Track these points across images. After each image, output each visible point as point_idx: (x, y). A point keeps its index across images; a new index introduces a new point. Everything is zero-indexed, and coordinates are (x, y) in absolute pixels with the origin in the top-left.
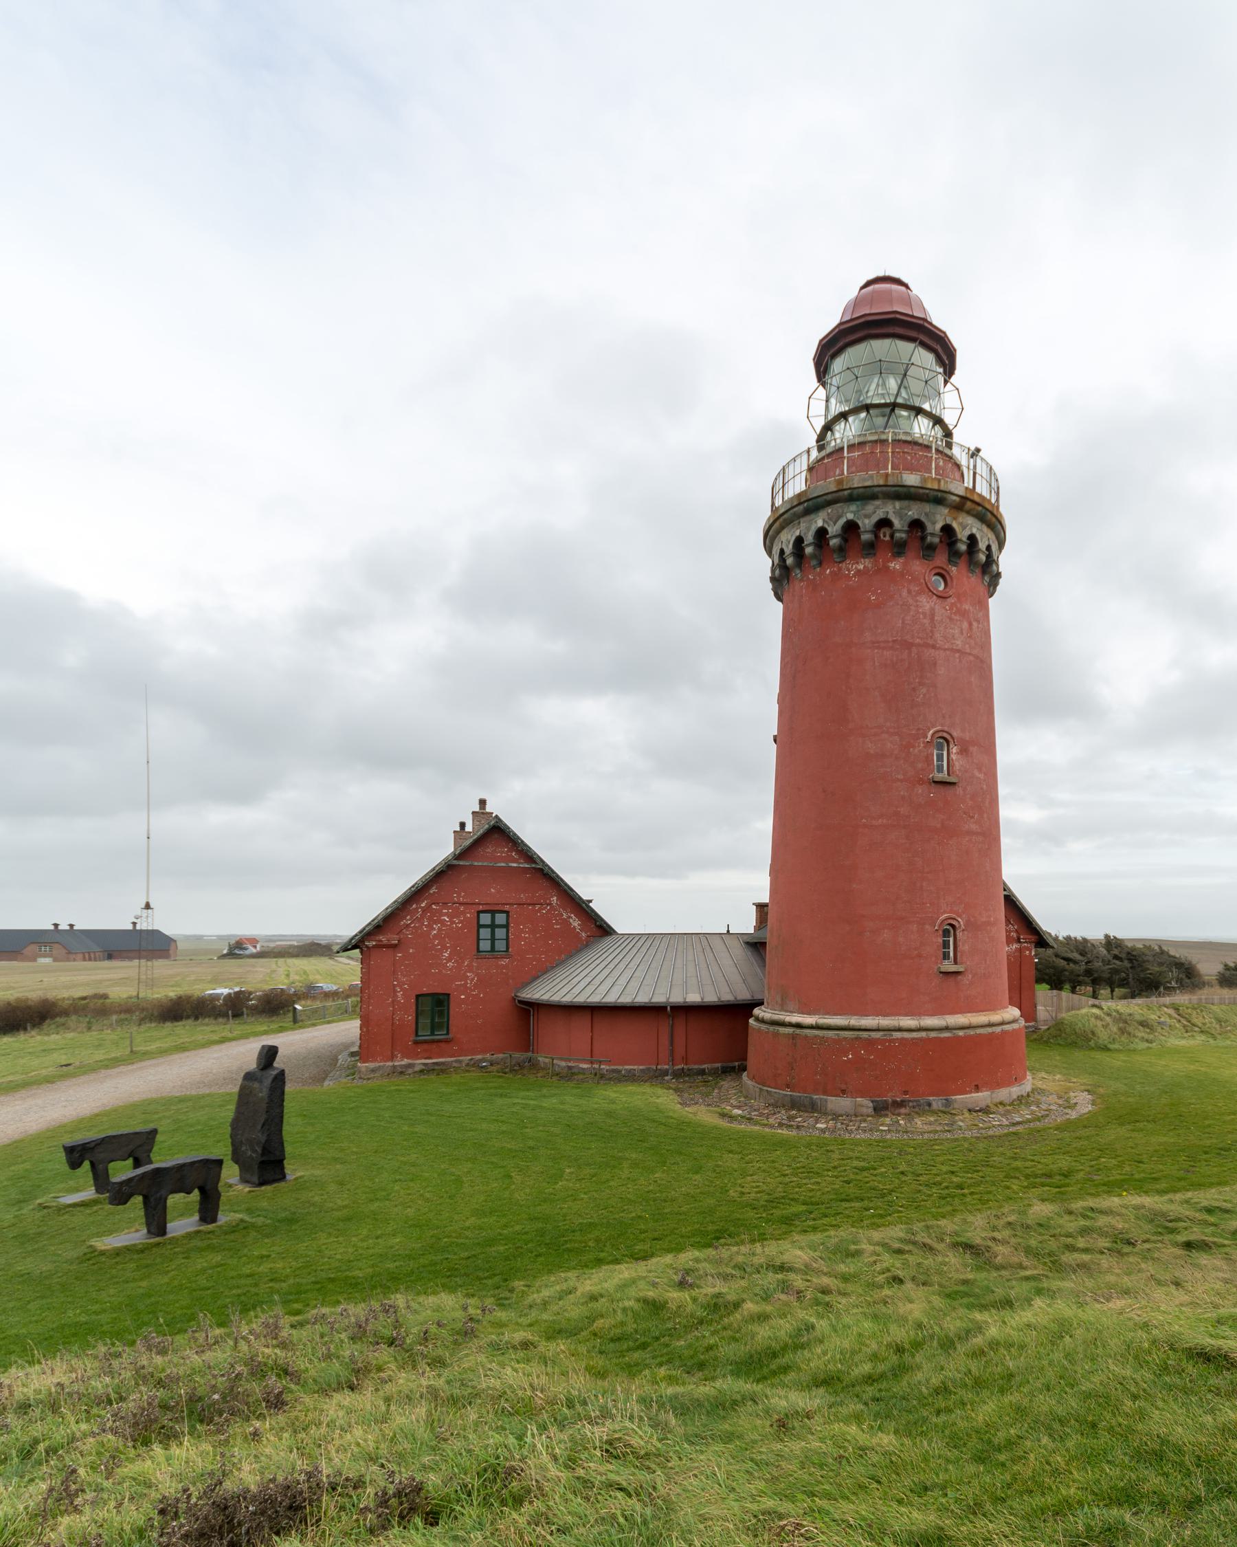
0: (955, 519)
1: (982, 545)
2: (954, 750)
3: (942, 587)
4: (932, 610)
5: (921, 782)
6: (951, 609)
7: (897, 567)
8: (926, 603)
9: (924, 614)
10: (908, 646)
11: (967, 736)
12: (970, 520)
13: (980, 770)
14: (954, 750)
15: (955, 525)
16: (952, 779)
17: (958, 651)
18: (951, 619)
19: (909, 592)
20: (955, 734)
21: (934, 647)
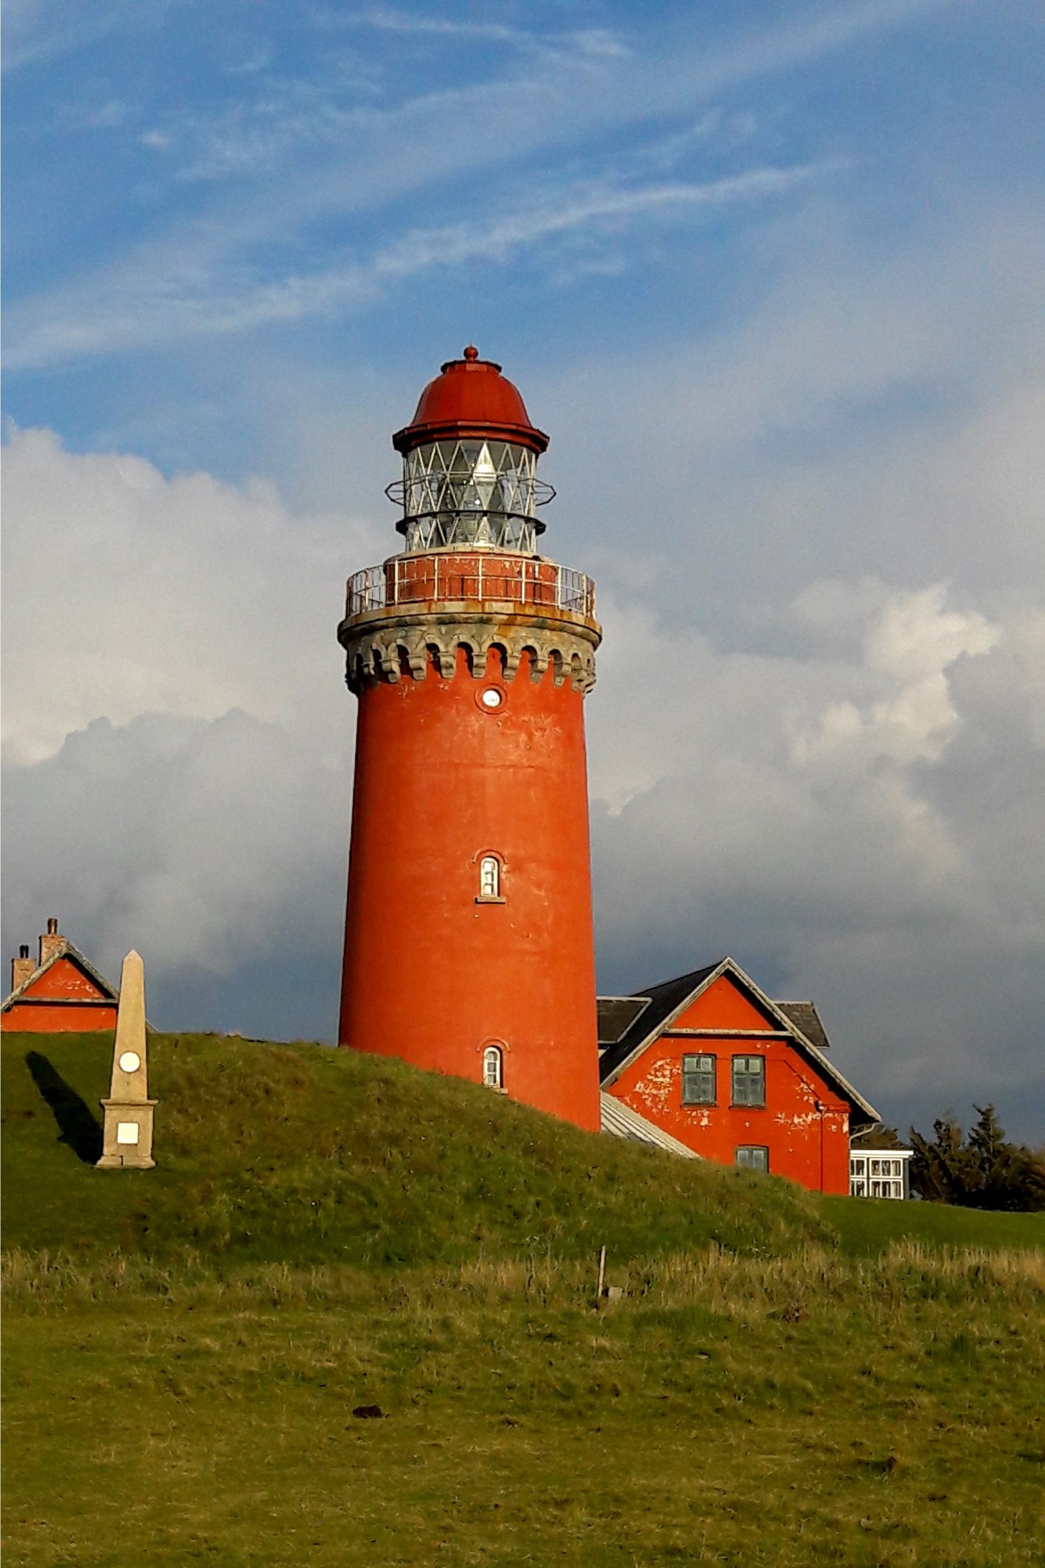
0: (505, 637)
1: (543, 654)
2: (505, 868)
4: (482, 729)
5: (465, 904)
6: (505, 723)
7: (446, 688)
8: (475, 722)
9: (473, 734)
10: (457, 766)
11: (522, 853)
12: (523, 632)
13: (539, 886)
14: (505, 868)
15: (504, 642)
16: (499, 900)
17: (512, 766)
18: (502, 734)
19: (458, 712)
20: (505, 853)
21: (482, 766)
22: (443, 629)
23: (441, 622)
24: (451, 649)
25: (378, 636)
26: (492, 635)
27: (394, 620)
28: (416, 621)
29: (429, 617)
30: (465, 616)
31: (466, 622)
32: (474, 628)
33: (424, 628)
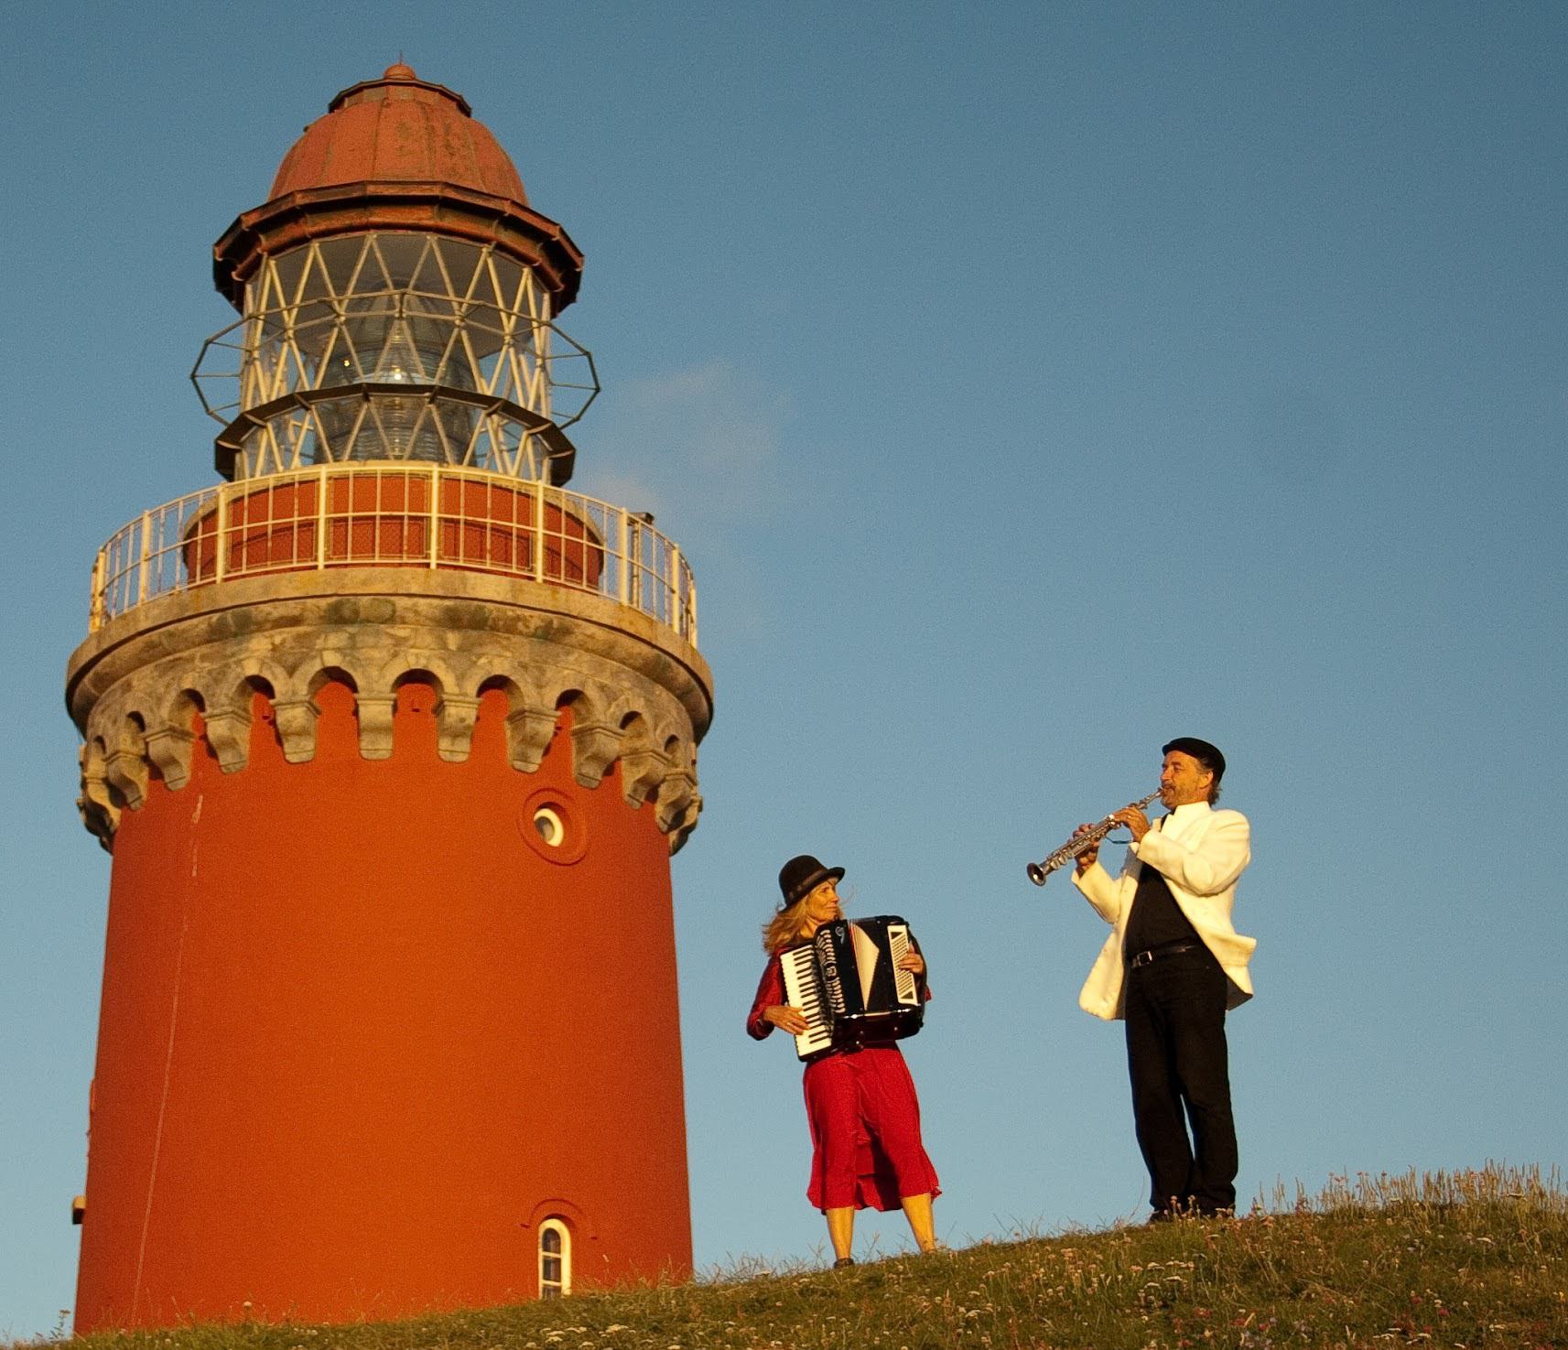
3: (556, 837)
15: (591, 692)
22: (453, 639)
23: (452, 620)
24: (472, 687)
25: (259, 645)
26: (569, 671)
27: (323, 603)
28: (387, 611)
29: (422, 601)
30: (510, 612)
31: (510, 628)
32: (524, 648)
33: (401, 632)
